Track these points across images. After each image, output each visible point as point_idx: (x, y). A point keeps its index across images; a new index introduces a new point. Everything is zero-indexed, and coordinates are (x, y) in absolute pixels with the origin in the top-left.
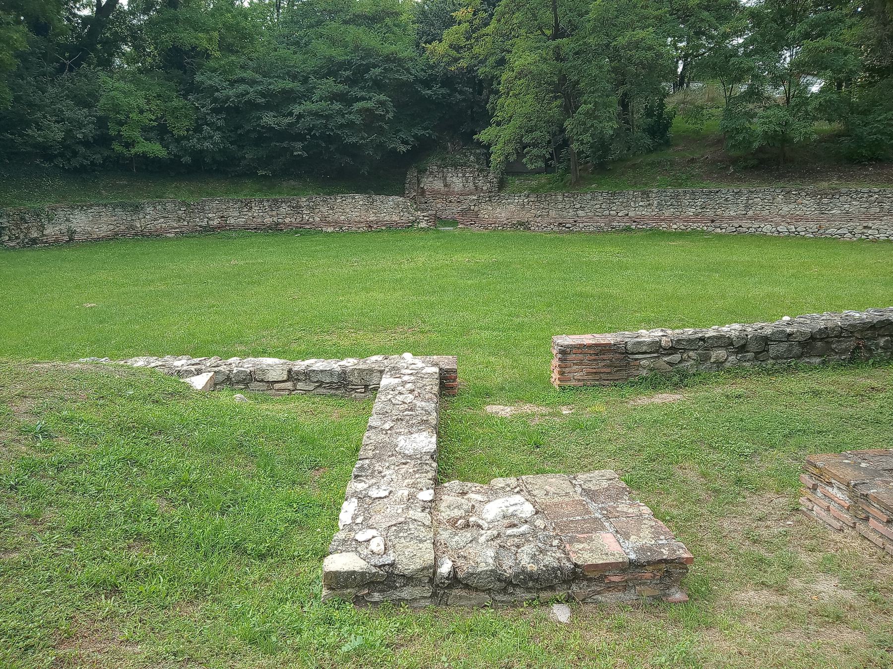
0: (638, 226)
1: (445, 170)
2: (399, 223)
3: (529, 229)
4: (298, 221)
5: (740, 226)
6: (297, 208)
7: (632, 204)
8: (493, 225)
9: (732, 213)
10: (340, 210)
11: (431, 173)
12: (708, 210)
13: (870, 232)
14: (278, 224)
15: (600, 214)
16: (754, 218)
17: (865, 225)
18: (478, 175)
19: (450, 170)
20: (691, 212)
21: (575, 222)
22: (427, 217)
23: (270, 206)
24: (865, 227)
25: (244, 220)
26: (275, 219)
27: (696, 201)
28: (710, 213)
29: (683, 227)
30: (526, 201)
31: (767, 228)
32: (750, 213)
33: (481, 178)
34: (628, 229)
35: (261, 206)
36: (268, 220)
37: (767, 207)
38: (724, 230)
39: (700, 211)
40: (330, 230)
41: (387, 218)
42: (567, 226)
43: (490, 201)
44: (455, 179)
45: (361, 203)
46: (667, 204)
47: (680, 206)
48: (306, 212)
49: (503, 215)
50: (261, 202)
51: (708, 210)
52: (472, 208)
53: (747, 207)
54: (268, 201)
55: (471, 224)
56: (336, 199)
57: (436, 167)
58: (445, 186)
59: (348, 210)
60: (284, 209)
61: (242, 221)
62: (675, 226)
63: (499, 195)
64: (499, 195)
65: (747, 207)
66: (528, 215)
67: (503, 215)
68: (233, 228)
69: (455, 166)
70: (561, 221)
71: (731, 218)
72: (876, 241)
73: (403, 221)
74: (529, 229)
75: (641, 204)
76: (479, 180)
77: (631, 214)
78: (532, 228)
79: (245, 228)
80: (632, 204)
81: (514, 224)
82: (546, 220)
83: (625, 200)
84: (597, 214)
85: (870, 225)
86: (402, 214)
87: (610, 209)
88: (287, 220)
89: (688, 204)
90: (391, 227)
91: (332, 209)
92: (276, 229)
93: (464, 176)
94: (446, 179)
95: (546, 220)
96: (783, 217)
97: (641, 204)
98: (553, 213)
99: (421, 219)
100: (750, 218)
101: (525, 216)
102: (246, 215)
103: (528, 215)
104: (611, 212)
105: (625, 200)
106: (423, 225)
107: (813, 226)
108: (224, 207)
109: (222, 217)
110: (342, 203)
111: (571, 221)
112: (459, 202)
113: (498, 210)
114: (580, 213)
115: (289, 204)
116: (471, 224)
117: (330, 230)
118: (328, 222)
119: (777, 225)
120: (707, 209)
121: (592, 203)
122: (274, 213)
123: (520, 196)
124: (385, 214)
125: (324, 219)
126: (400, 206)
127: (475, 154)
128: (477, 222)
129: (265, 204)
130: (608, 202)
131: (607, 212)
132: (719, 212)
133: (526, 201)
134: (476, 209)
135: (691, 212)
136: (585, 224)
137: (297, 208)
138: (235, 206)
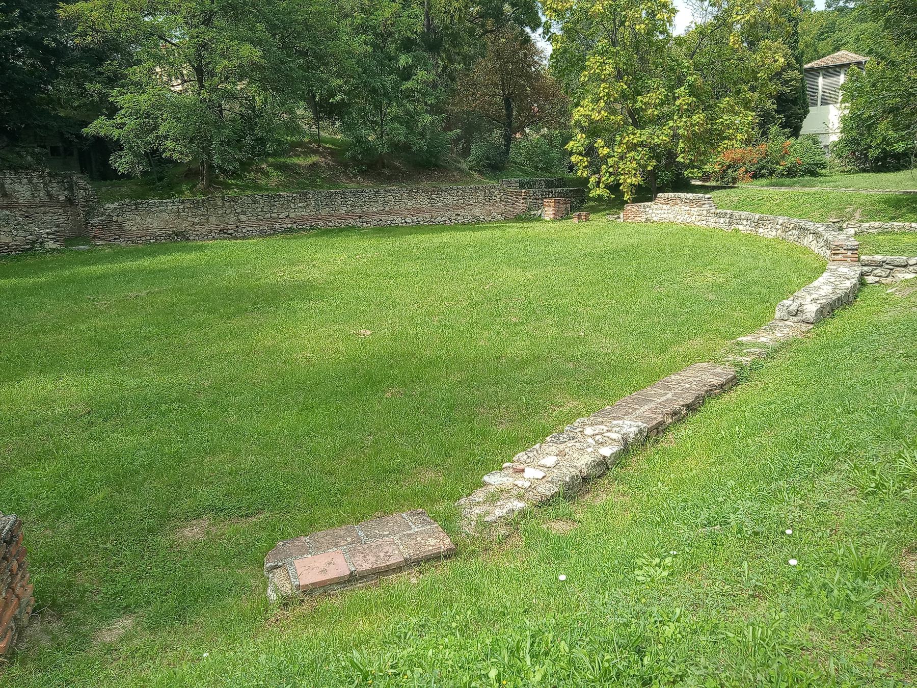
0: (299, 227)
2: (12, 246)
3: (188, 239)
5: (381, 220)
7: (292, 205)
13: (459, 217)
17: (456, 213)
18: (50, 181)
20: (343, 209)
21: (237, 227)
22: (52, 234)
28: (358, 211)
29: (337, 225)
30: (181, 207)
31: (399, 220)
32: (387, 208)
34: (291, 230)
37: (398, 203)
42: (229, 232)
43: (136, 209)
44: (17, 187)
49: (155, 225)
52: (115, 218)
55: (115, 239)
62: (330, 224)
63: (147, 202)
64: (147, 202)
66: (185, 223)
67: (155, 225)
69: (15, 169)
70: (223, 227)
71: (374, 213)
72: (463, 224)
73: (18, 243)
74: (188, 239)
75: (300, 205)
76: (52, 187)
77: (292, 215)
78: (191, 238)
80: (292, 205)
82: (207, 227)
84: (259, 217)
85: (459, 213)
86: (15, 233)
93: (30, 182)
95: (207, 227)
97: (300, 205)
98: (213, 220)
99: (45, 238)
100: (387, 213)
101: (182, 225)
104: (273, 215)
105: (285, 202)
106: (51, 245)
107: (428, 216)
111: (234, 226)
112: (27, 216)
113: (148, 220)
114: (242, 217)
116: (115, 239)
119: (405, 217)
123: (173, 203)
126: (11, 222)
127: (33, 154)
128: (123, 236)
130: (269, 204)
133: (181, 207)
134: (120, 219)
135: (343, 209)
136: (248, 229)
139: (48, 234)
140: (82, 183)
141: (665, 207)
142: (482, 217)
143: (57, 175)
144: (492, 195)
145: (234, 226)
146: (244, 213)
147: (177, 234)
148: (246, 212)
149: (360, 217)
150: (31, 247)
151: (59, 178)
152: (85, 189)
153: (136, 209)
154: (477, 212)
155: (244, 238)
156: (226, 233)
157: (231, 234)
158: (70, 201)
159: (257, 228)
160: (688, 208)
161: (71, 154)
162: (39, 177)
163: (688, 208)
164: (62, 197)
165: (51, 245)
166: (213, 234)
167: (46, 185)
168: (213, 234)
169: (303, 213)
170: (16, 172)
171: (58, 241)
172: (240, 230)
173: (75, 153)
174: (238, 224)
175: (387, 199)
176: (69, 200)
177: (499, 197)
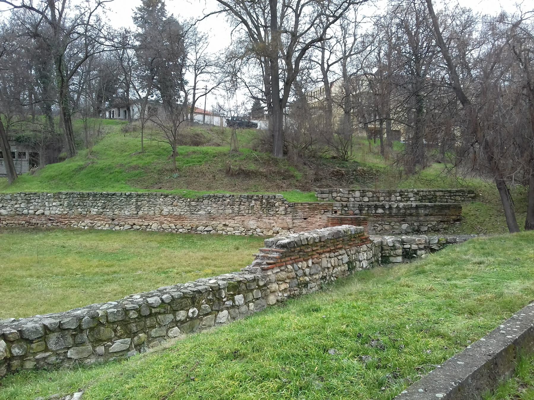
0: (54, 224)
5: (134, 224)
7: (47, 203)
9: (127, 213)
12: (108, 210)
13: (228, 229)
15: (21, 213)
16: (142, 217)
17: (224, 223)
20: (94, 211)
24: (225, 225)
27: (97, 202)
28: (110, 213)
37: (152, 208)
38: (122, 228)
39: (101, 210)
46: (75, 204)
47: (85, 207)
51: (108, 210)
53: (138, 208)
65: (138, 208)
75: (54, 204)
77: (47, 213)
83: (40, 201)
84: (18, 212)
85: (227, 223)
89: (91, 204)
96: (165, 216)
97: (54, 204)
100: (141, 217)
119: (162, 223)
120: (107, 209)
121: (13, 202)
131: (25, 211)
132: (117, 212)
135: (94, 211)
148: (6, 207)
149: (113, 220)
154: (252, 223)
159: (16, 222)
169: (57, 212)
175: (139, 203)
177: (282, 208)
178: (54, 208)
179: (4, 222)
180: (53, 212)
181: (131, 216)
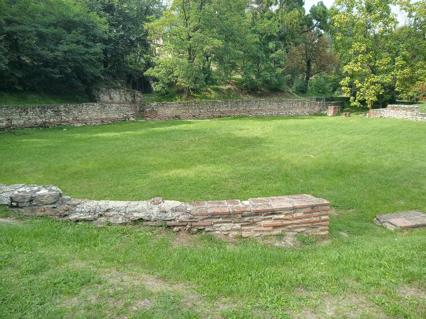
1: (110, 90)
3: (180, 119)
4: (58, 120)
6: (57, 113)
7: (221, 106)
8: (164, 118)
10: (86, 113)
11: (102, 92)
13: (290, 113)
14: (45, 123)
18: (127, 93)
19: (112, 90)
20: (241, 109)
23: (40, 111)
25: (23, 121)
26: (44, 120)
28: (248, 109)
29: (239, 115)
31: (264, 114)
32: (260, 108)
33: (128, 95)
34: (220, 117)
35: (34, 111)
36: (39, 121)
40: (79, 125)
41: (112, 116)
42: (196, 116)
43: (163, 106)
44: (115, 95)
45: (98, 108)
48: (64, 114)
49: (169, 112)
50: (34, 108)
53: (259, 106)
54: (38, 107)
56: (83, 106)
57: (105, 89)
58: (111, 99)
59: (90, 113)
60: (50, 113)
61: (22, 122)
62: (236, 115)
65: (259, 106)
66: (180, 112)
67: (169, 112)
68: (16, 128)
69: (115, 88)
70: (194, 114)
71: (254, 110)
72: (292, 116)
73: (120, 118)
74: (180, 119)
75: (224, 106)
78: (182, 118)
79: (22, 127)
80: (221, 106)
81: (174, 117)
82: (188, 114)
86: (120, 114)
87: (213, 108)
88: (52, 120)
90: (114, 121)
91: (81, 112)
92: (44, 126)
93: (120, 94)
94: (110, 95)
97: (224, 106)
98: (190, 111)
100: (259, 111)
101: (179, 113)
102: (24, 117)
103: (180, 112)
104: (214, 110)
105: (219, 105)
106: (132, 119)
107: (277, 112)
108: (10, 112)
109: (9, 120)
110: (87, 108)
111: (198, 114)
114: (202, 111)
115: (52, 109)
117: (79, 125)
118: (78, 120)
119: (267, 113)
122: (43, 116)
124: (111, 114)
125: (76, 119)
127: (121, 83)
129: (37, 109)
133: (179, 105)
134: (157, 110)
136: (204, 115)
137: (57, 113)
138: (17, 111)
139: (131, 114)
140: (139, 94)
141: (392, 111)
142: (299, 113)
143: (129, 91)
144: (304, 104)
145: (198, 114)
146: (202, 109)
147: (177, 116)
150: (125, 120)
151: (130, 92)
152: (140, 97)
153: (163, 106)
154: (298, 111)
155: (202, 119)
156: (195, 117)
157: (197, 117)
158: (133, 102)
160: (405, 112)
161: (130, 83)
162: (123, 92)
163: (405, 112)
164: (130, 100)
165: (132, 119)
166: (190, 117)
167: (125, 95)
168: (190, 117)
169: (225, 109)
170: (115, 89)
171: (134, 118)
172: (200, 116)
173: (131, 82)
174: (200, 113)
175: (260, 104)
176: (133, 101)
178: (225, 108)
179: (202, 116)
180: (224, 110)
181: (256, 110)
